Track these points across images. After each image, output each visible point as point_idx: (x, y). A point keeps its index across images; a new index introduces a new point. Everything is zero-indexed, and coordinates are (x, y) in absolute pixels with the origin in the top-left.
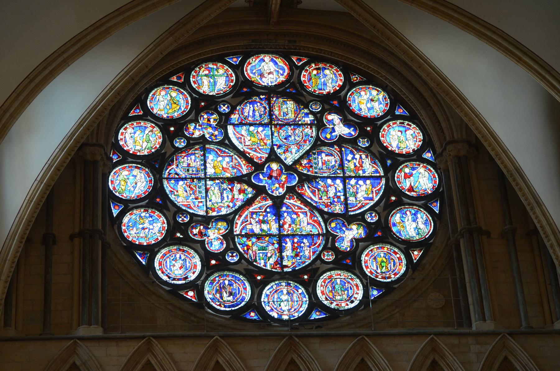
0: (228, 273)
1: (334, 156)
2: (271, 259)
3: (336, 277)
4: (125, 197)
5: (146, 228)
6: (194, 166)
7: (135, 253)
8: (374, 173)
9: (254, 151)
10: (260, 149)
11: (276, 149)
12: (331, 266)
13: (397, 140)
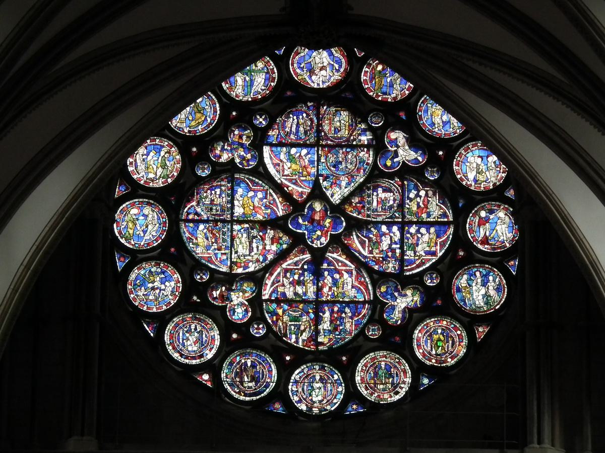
0: (251, 351)
1: (393, 192)
2: (304, 334)
3: (380, 359)
4: (132, 245)
5: (157, 288)
6: (218, 203)
7: (142, 321)
8: (441, 218)
9: (294, 184)
10: (302, 181)
11: (321, 181)
12: (376, 344)
13: (475, 170)
